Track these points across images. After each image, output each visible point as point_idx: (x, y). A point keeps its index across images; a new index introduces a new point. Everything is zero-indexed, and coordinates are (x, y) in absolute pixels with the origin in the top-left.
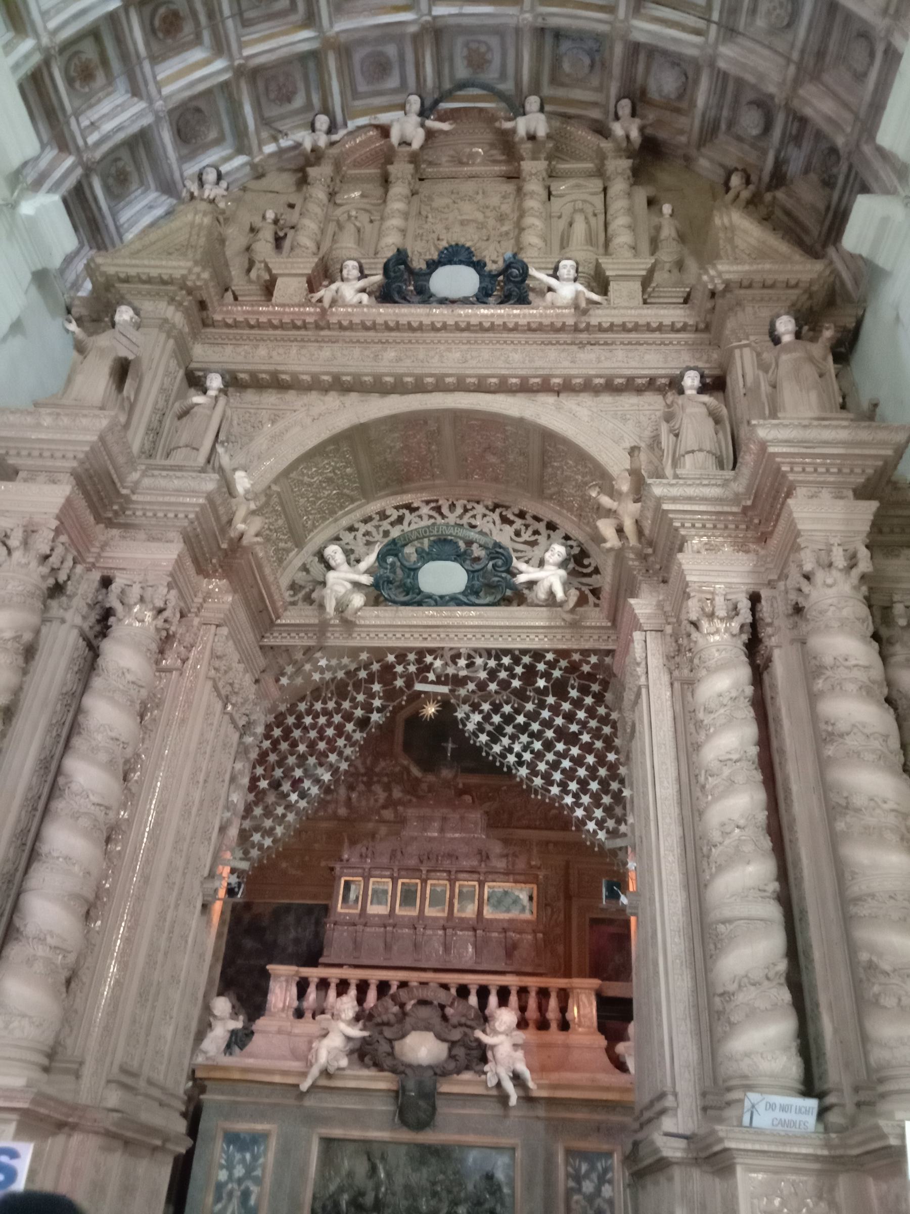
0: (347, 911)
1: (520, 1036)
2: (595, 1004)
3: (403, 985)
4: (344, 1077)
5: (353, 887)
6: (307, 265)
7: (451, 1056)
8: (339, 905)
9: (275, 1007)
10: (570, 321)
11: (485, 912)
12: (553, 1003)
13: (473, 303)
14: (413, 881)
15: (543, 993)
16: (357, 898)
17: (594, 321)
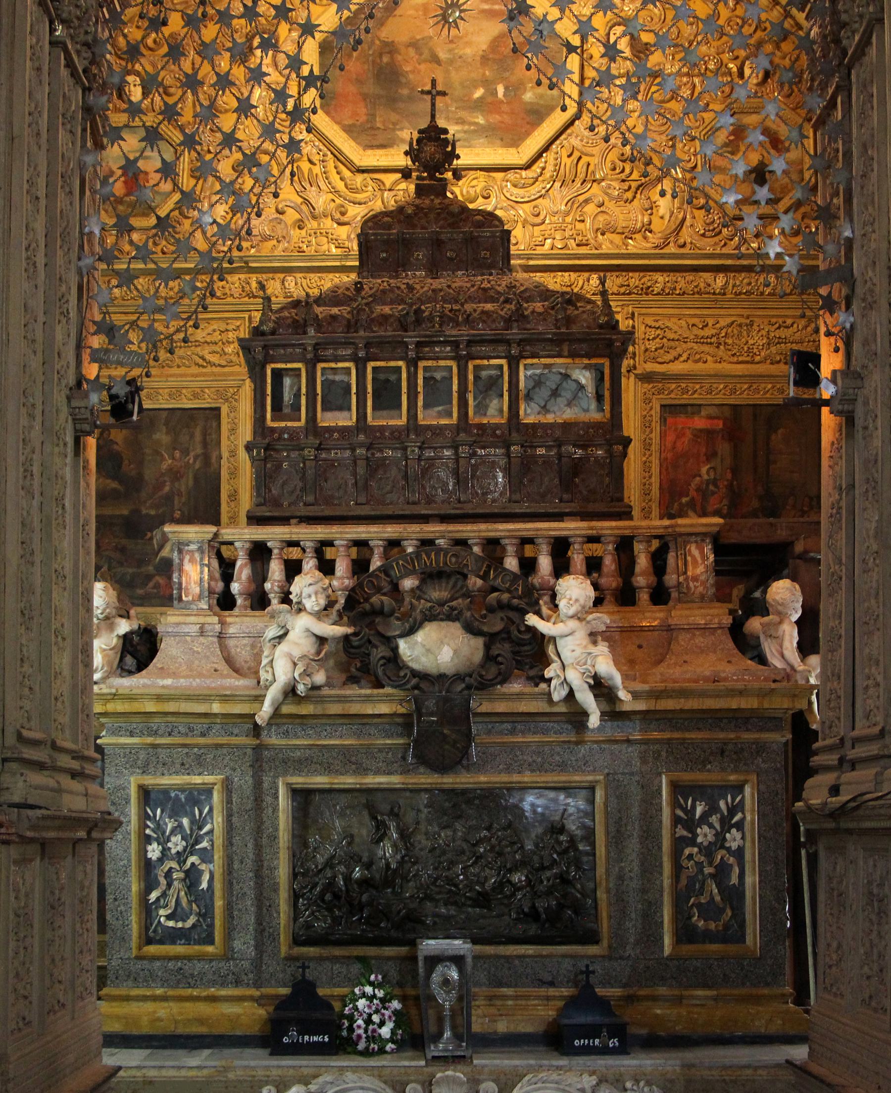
0: (283, 424)
3: (393, 544)
4: (322, 700)
5: (287, 381)
8: (269, 415)
14: (392, 364)
15: (625, 545)
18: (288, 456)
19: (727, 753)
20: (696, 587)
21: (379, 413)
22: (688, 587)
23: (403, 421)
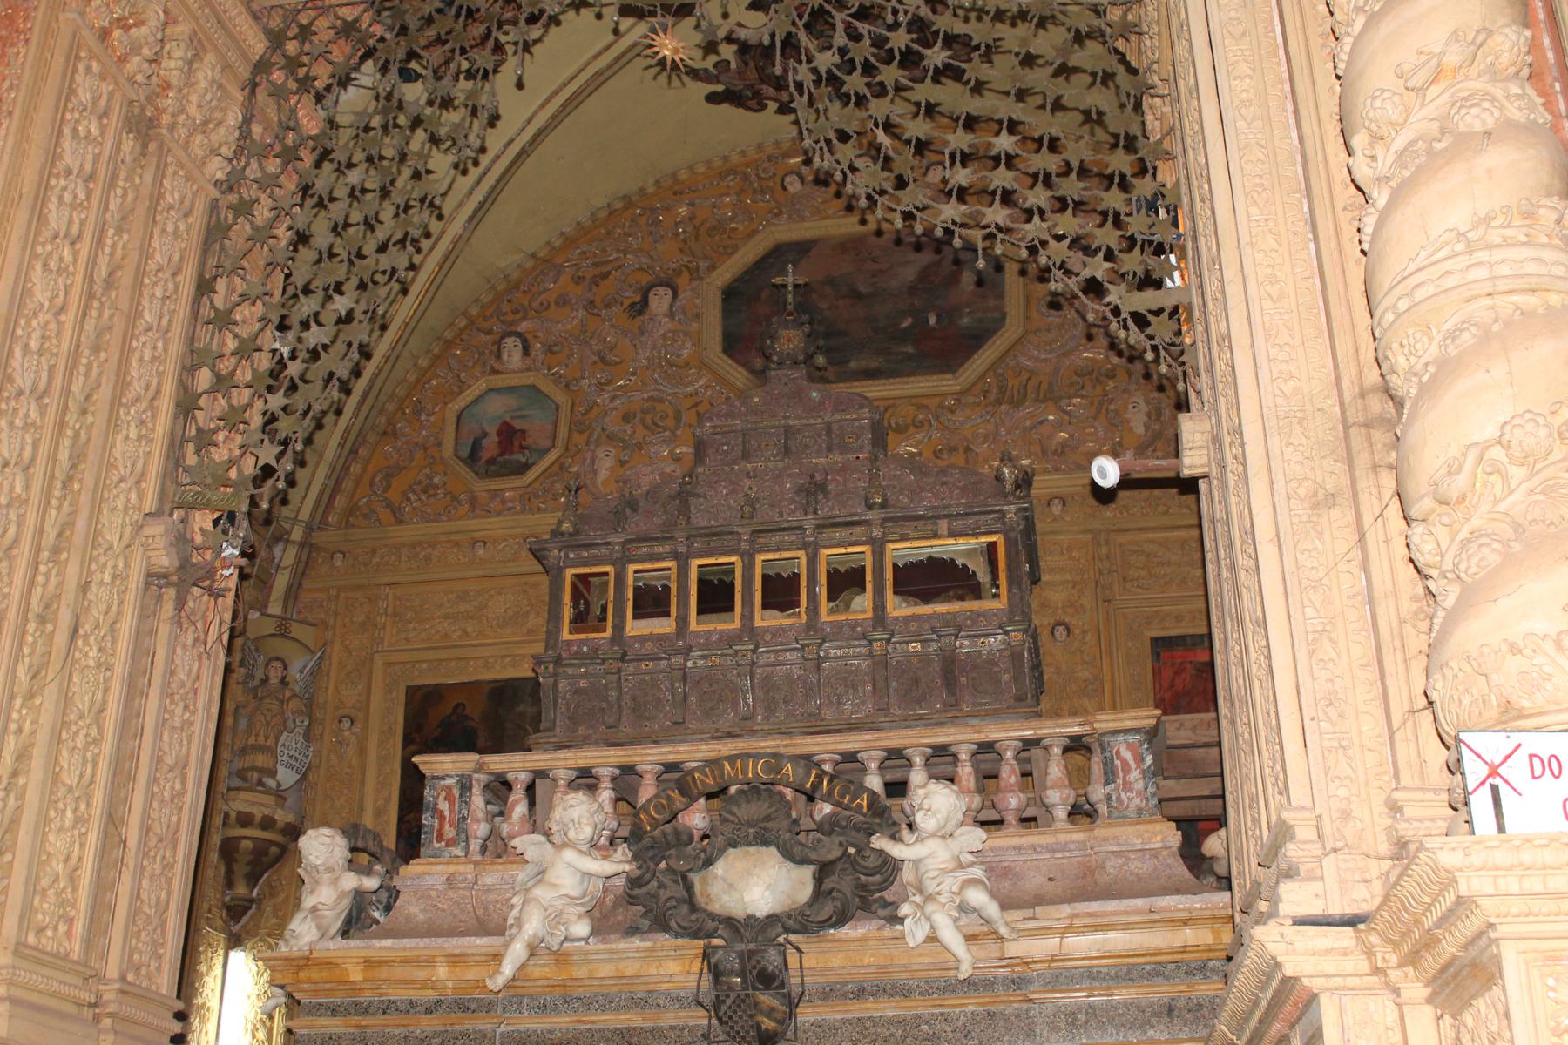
1: (975, 837)
2: (1149, 760)
7: (819, 894)
9: (440, 837)
11: (889, 606)
12: (1056, 770)
16: (604, 609)
18: (586, 671)
19: (1176, 1013)
20: (1130, 799)
21: (704, 617)
22: (1119, 799)
23: (737, 624)
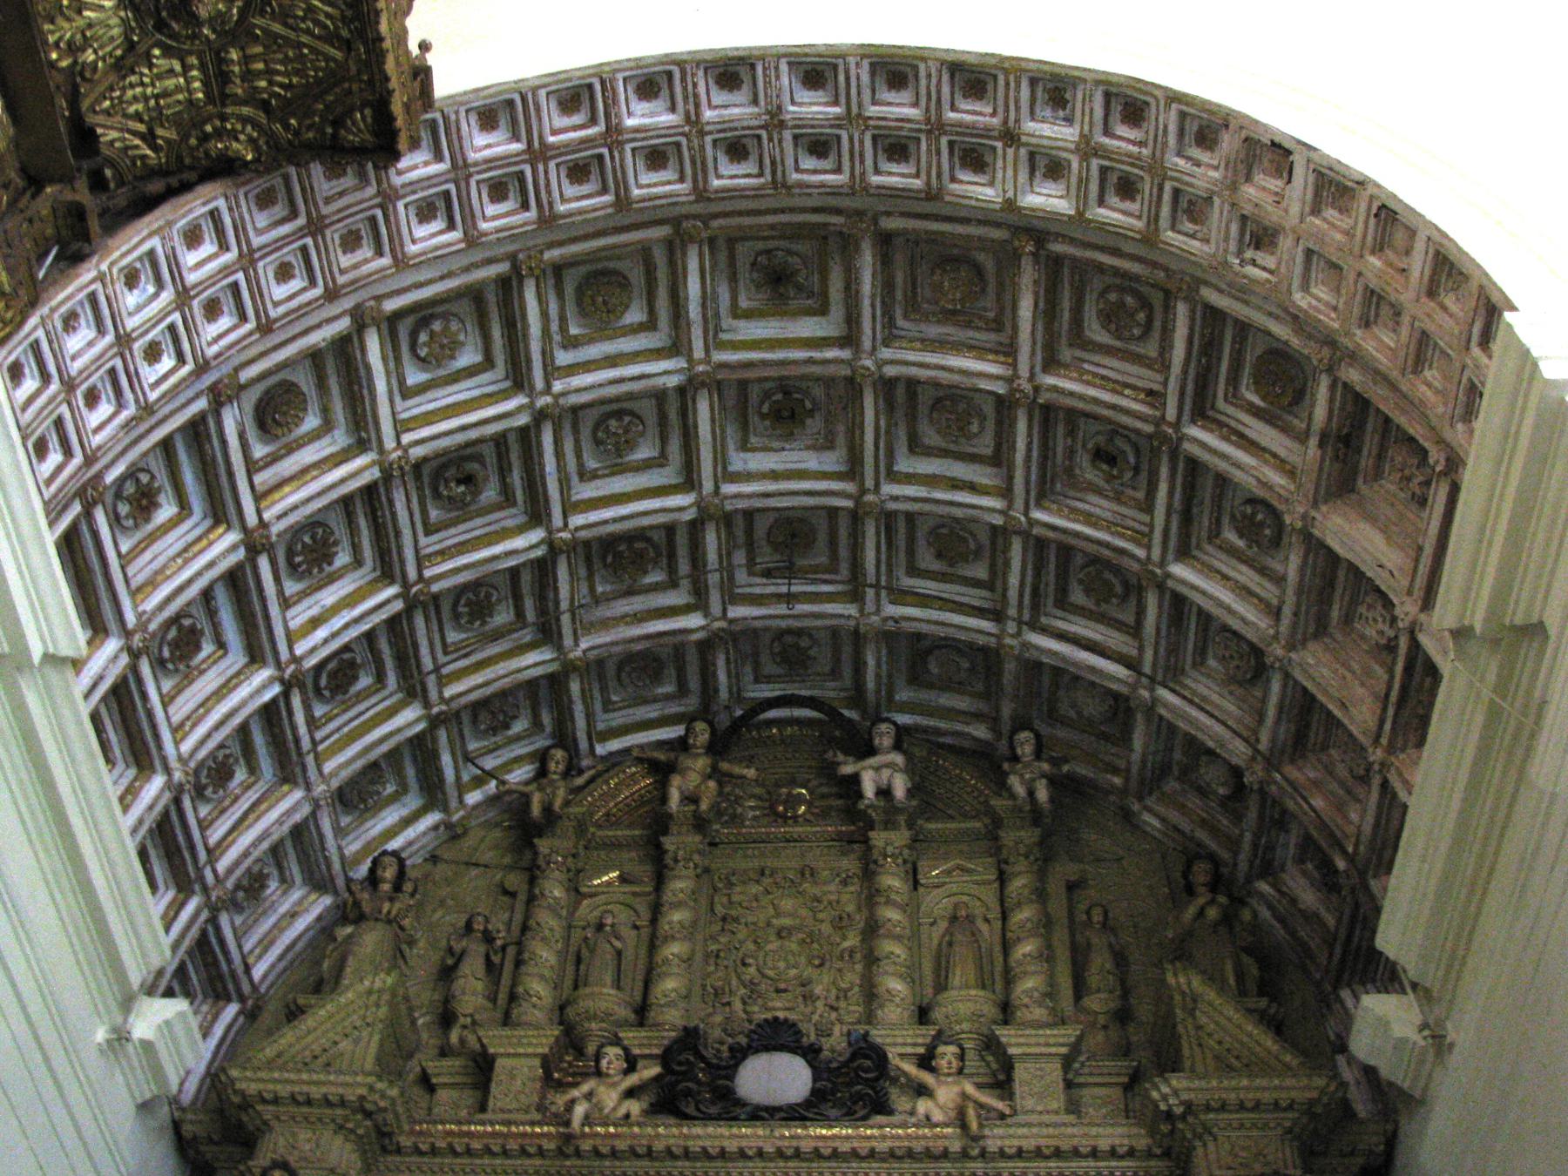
6: (544, 1039)
10: (956, 1146)
13: (804, 1119)
17: (992, 1145)
